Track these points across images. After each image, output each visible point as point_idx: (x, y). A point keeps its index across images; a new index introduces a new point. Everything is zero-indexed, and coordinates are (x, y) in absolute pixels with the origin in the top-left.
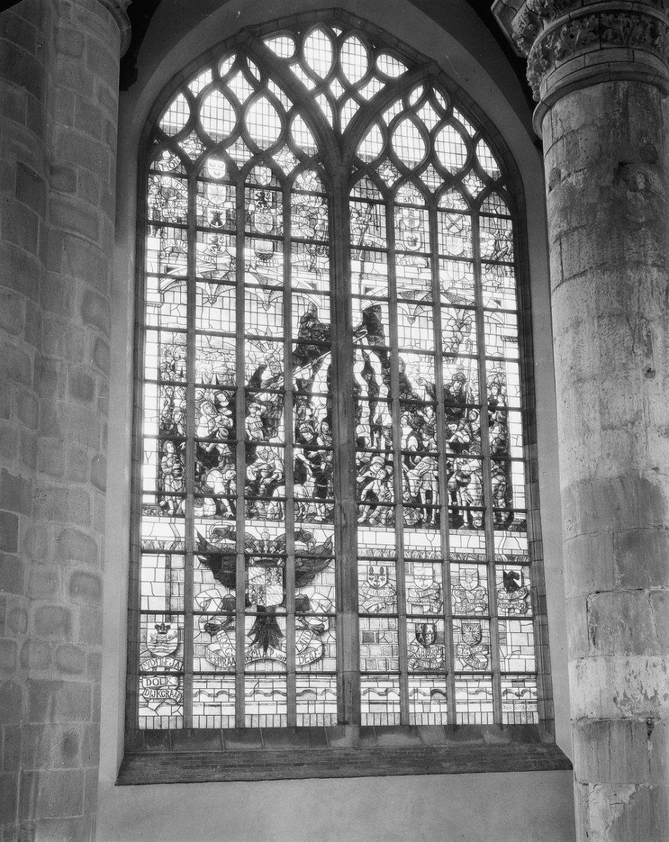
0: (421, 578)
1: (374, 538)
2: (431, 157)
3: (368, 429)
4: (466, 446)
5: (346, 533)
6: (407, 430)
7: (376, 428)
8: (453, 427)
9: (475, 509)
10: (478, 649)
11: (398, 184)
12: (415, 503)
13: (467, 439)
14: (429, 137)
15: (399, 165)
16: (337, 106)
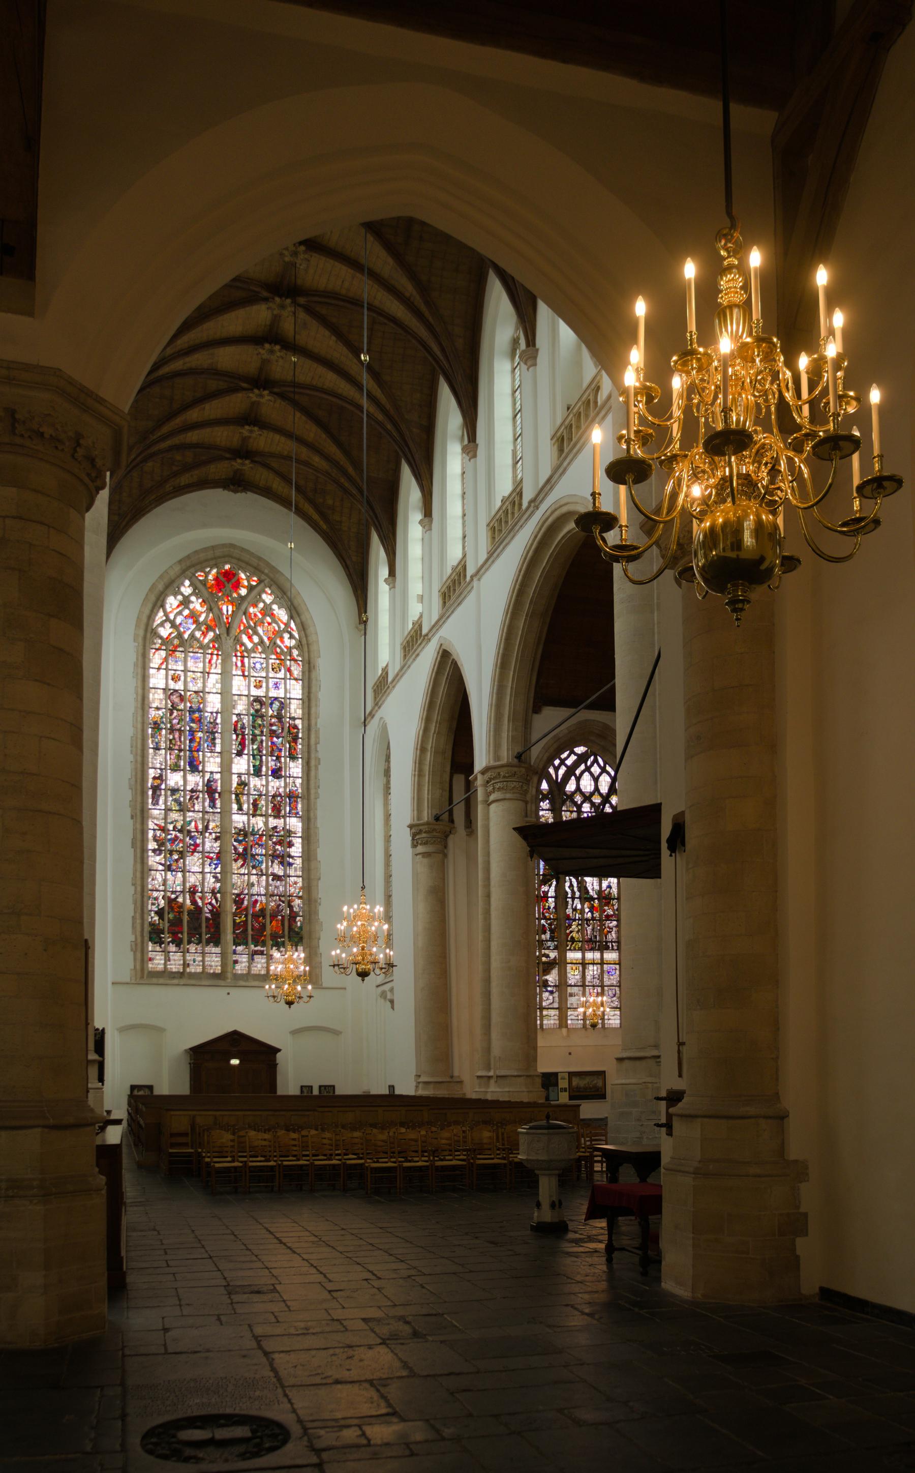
0: (592, 971)
1: (574, 955)
2: (597, 789)
3: (571, 910)
4: (612, 916)
5: (563, 956)
6: (587, 910)
7: (575, 910)
8: (606, 908)
9: (614, 942)
10: (614, 998)
11: (583, 802)
12: (590, 940)
13: (612, 913)
14: (596, 780)
15: (582, 794)
16: (557, 769)
